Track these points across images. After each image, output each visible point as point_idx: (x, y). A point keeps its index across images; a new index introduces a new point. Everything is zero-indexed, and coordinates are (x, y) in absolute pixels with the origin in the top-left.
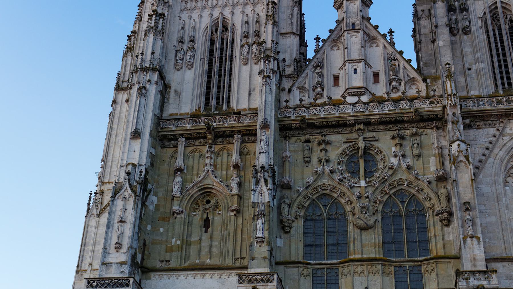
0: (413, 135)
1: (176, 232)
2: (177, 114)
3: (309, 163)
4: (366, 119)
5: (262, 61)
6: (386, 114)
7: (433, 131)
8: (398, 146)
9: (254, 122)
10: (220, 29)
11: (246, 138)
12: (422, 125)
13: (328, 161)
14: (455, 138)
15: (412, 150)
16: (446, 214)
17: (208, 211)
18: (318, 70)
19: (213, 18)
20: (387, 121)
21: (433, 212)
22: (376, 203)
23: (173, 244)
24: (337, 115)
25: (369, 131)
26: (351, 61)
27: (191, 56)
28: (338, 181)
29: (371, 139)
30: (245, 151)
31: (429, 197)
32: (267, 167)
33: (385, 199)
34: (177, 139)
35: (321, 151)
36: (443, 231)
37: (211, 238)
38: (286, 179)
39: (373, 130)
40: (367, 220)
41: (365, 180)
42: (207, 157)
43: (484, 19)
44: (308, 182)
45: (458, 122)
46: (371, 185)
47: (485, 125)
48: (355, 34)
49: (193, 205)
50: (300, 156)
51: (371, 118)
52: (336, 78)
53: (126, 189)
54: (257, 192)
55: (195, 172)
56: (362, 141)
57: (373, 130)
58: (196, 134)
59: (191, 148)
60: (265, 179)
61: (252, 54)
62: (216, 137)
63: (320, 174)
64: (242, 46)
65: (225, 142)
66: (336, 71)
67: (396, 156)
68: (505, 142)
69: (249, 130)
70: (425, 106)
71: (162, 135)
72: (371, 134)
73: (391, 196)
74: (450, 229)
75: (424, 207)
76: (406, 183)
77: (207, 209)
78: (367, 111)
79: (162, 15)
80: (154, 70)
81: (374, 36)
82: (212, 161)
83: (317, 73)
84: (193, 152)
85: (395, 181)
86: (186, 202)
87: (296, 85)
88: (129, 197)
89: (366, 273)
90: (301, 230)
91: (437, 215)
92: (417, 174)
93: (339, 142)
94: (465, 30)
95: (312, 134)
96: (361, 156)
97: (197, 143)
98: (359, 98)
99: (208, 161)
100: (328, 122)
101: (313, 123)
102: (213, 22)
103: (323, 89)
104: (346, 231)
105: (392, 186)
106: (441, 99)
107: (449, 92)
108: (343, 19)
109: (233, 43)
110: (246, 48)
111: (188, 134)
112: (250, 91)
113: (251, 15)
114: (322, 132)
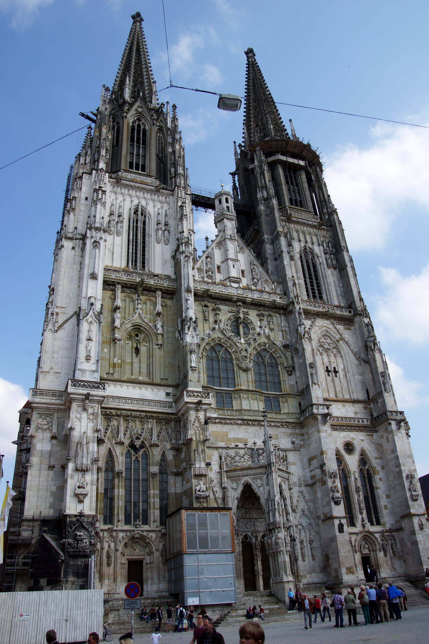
0: (270, 315)
1: (117, 353)
2: (112, 267)
11: (165, 295)
13: (220, 321)
18: (209, 260)
24: (227, 293)
25: (244, 307)
26: (232, 260)
30: (164, 304)
34: (115, 286)
37: (140, 362)
42: (138, 304)
52: (219, 267)
55: (127, 312)
59: (124, 294)
66: (219, 264)
67: (261, 327)
69: (168, 290)
72: (246, 310)
77: (137, 340)
89: (250, 399)
93: (225, 311)
95: (208, 301)
96: (241, 323)
97: (128, 292)
101: (212, 295)
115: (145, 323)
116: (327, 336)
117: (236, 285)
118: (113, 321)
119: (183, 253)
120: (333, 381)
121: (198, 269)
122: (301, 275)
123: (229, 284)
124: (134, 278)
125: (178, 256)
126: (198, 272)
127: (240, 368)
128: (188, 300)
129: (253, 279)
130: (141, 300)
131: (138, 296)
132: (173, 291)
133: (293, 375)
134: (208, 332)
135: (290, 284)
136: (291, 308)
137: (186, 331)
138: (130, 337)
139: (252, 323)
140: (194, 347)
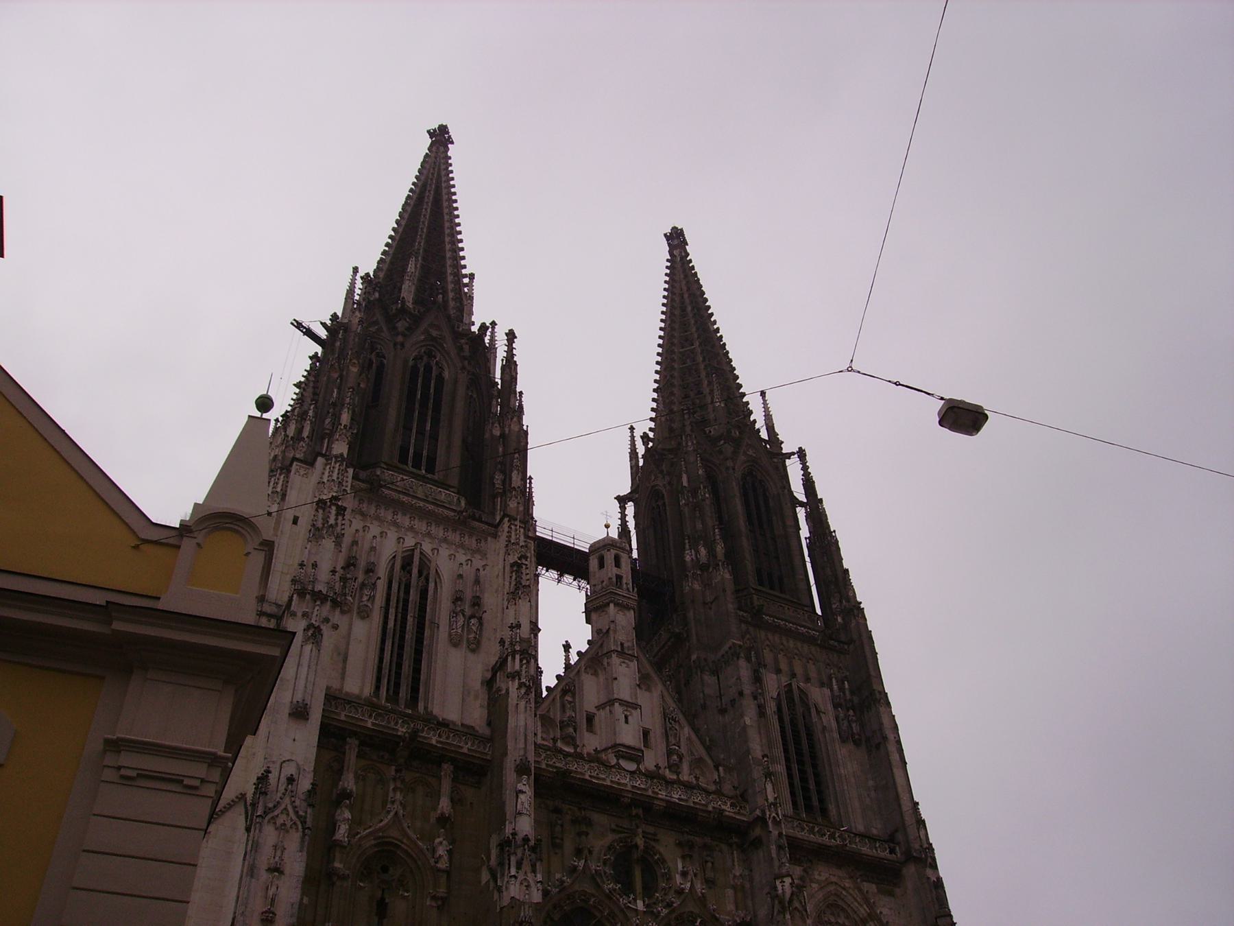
2: (340, 690)
5: (518, 657)
6: (675, 803)
10: (415, 571)
13: (590, 852)
15: (704, 872)
18: (568, 698)
26: (623, 703)
28: (607, 891)
42: (394, 790)
43: (778, 700)
48: (627, 661)
51: (655, 802)
52: (590, 719)
53: (286, 809)
54: (518, 882)
64: (454, 614)
66: (593, 710)
67: (684, 874)
70: (723, 807)
72: (651, 829)
76: (699, 920)
78: (650, 790)
83: (570, 703)
85: (684, 913)
92: (714, 910)
98: (638, 765)
99: (399, 796)
108: (608, 631)
115: (409, 838)
117: (632, 766)
118: (332, 827)
119: (514, 675)
121: (543, 717)
122: (779, 752)
123: (613, 761)
124: (392, 725)
125: (501, 682)
126: (543, 725)
128: (522, 792)
129: (670, 753)
130: (403, 781)
131: (397, 771)
134: (558, 876)
135: (757, 773)
136: (757, 831)
137: (513, 872)
139: (664, 861)
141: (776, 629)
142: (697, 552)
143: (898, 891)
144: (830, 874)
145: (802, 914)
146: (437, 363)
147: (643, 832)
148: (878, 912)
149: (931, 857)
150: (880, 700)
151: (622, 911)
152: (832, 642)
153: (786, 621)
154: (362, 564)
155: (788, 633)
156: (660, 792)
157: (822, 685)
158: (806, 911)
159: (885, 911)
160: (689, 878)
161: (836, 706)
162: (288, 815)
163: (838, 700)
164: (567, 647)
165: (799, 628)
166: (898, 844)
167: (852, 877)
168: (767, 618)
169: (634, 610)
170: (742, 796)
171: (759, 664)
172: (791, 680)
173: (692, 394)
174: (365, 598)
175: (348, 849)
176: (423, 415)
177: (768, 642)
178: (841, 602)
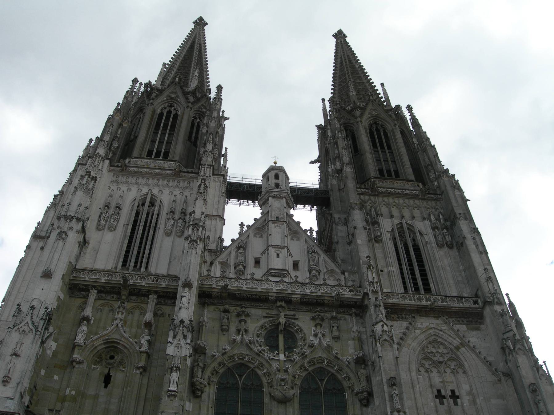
0: (333, 318)
2: (92, 268)
3: (226, 331)
4: (289, 297)
6: (307, 295)
7: (351, 317)
8: (319, 327)
9: (172, 285)
10: (147, 204)
11: (162, 300)
12: (342, 311)
13: (246, 331)
14: (378, 320)
15: (332, 332)
16: (366, 393)
17: (110, 367)
19: (141, 193)
20: (308, 302)
21: (353, 391)
22: (295, 378)
23: (66, 394)
24: (259, 290)
25: (289, 309)
26: (274, 247)
27: (115, 219)
29: (291, 317)
30: (159, 312)
31: (348, 377)
32: (187, 323)
33: (304, 374)
34: (88, 291)
35: (240, 322)
36: (362, 411)
38: (202, 343)
39: (293, 309)
40: (286, 393)
41: (285, 355)
44: (225, 349)
45: (380, 306)
46: (291, 360)
47: (399, 318)
48: (279, 225)
49: (94, 358)
50: (217, 325)
51: (293, 296)
52: (257, 262)
53: (27, 323)
54: (174, 345)
56: (283, 317)
57: (293, 309)
58: (110, 288)
59: (101, 302)
60: (183, 333)
61: (177, 227)
62: (131, 294)
63: (238, 343)
65: (139, 301)
66: (258, 255)
67: (316, 335)
68: (417, 335)
69: (167, 292)
70: (344, 293)
71: (73, 284)
73: (309, 373)
74: (369, 409)
75: (343, 387)
76: (326, 361)
77: (109, 364)
79: (94, 179)
80: (78, 220)
81: (296, 231)
82: (123, 316)
83: (241, 253)
84: (103, 305)
85: (314, 358)
86: (88, 353)
87: (219, 260)
88: (29, 332)
90: (213, 397)
91: (357, 394)
92: (336, 353)
94: (377, 239)
95: (231, 305)
96: (281, 331)
97: (109, 298)
100: (250, 295)
101: (235, 294)
102: (141, 196)
103: (244, 268)
104: (262, 403)
105: (312, 362)
106: (360, 289)
107: (371, 280)
108: (268, 212)
109: (157, 218)
110: (172, 222)
111: (101, 286)
112: (170, 259)
113: (179, 197)
114: (242, 305)
115: (125, 338)
116: (438, 342)
120: (450, 411)
127: (272, 397)
130: (124, 308)
132: (174, 293)
133: (370, 407)
136: (366, 302)
137: (170, 339)
138: (99, 359)
139: (301, 330)
140: (177, 362)
141: (389, 194)
142: (335, 165)
143: (482, 327)
144: (430, 324)
145: (390, 343)
146: (175, 109)
147: (285, 315)
148: (467, 341)
149: (497, 298)
150: (460, 218)
151: (267, 361)
152: (429, 196)
153: (395, 189)
154: (113, 205)
155: (398, 195)
156: (296, 290)
157: (424, 219)
158: (393, 340)
159: (473, 340)
160: (318, 336)
161: (434, 228)
162: (28, 326)
163: (434, 225)
164: (242, 225)
165: (404, 191)
166: (479, 298)
167: (446, 323)
168: (381, 189)
169: (285, 198)
170: (360, 287)
171: (377, 215)
172: (401, 220)
173: (344, 98)
174: (112, 220)
175: (83, 347)
176: (163, 134)
177: (384, 203)
178: (435, 173)
